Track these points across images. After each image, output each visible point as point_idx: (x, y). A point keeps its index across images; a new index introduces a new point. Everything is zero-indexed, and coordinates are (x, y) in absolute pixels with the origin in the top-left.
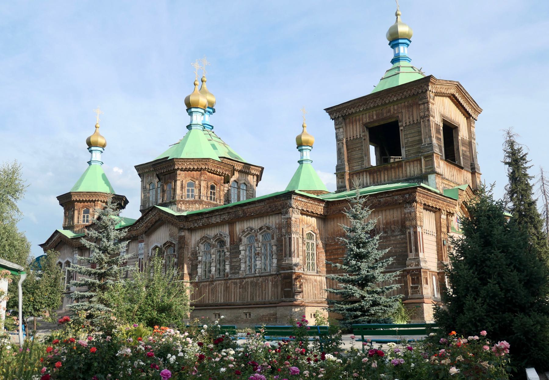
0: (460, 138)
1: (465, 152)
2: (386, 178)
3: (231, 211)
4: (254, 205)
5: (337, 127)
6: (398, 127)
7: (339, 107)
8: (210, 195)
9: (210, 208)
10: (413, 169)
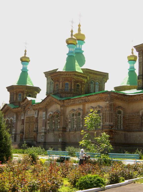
3: (83, 99)
4: (93, 97)
5: (139, 56)
7: (140, 46)
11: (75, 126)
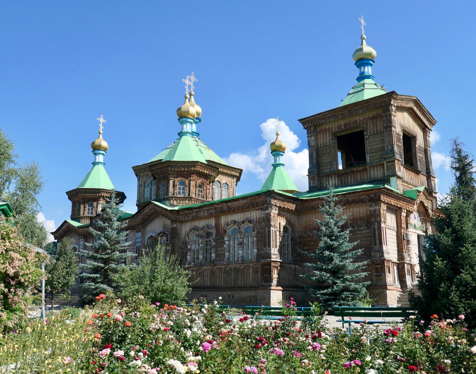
0: (417, 146)
1: (422, 157)
2: (352, 180)
3: (217, 206)
5: (309, 135)
6: (364, 136)
8: (198, 193)
9: (198, 204)
10: (376, 173)
11: (201, 257)
